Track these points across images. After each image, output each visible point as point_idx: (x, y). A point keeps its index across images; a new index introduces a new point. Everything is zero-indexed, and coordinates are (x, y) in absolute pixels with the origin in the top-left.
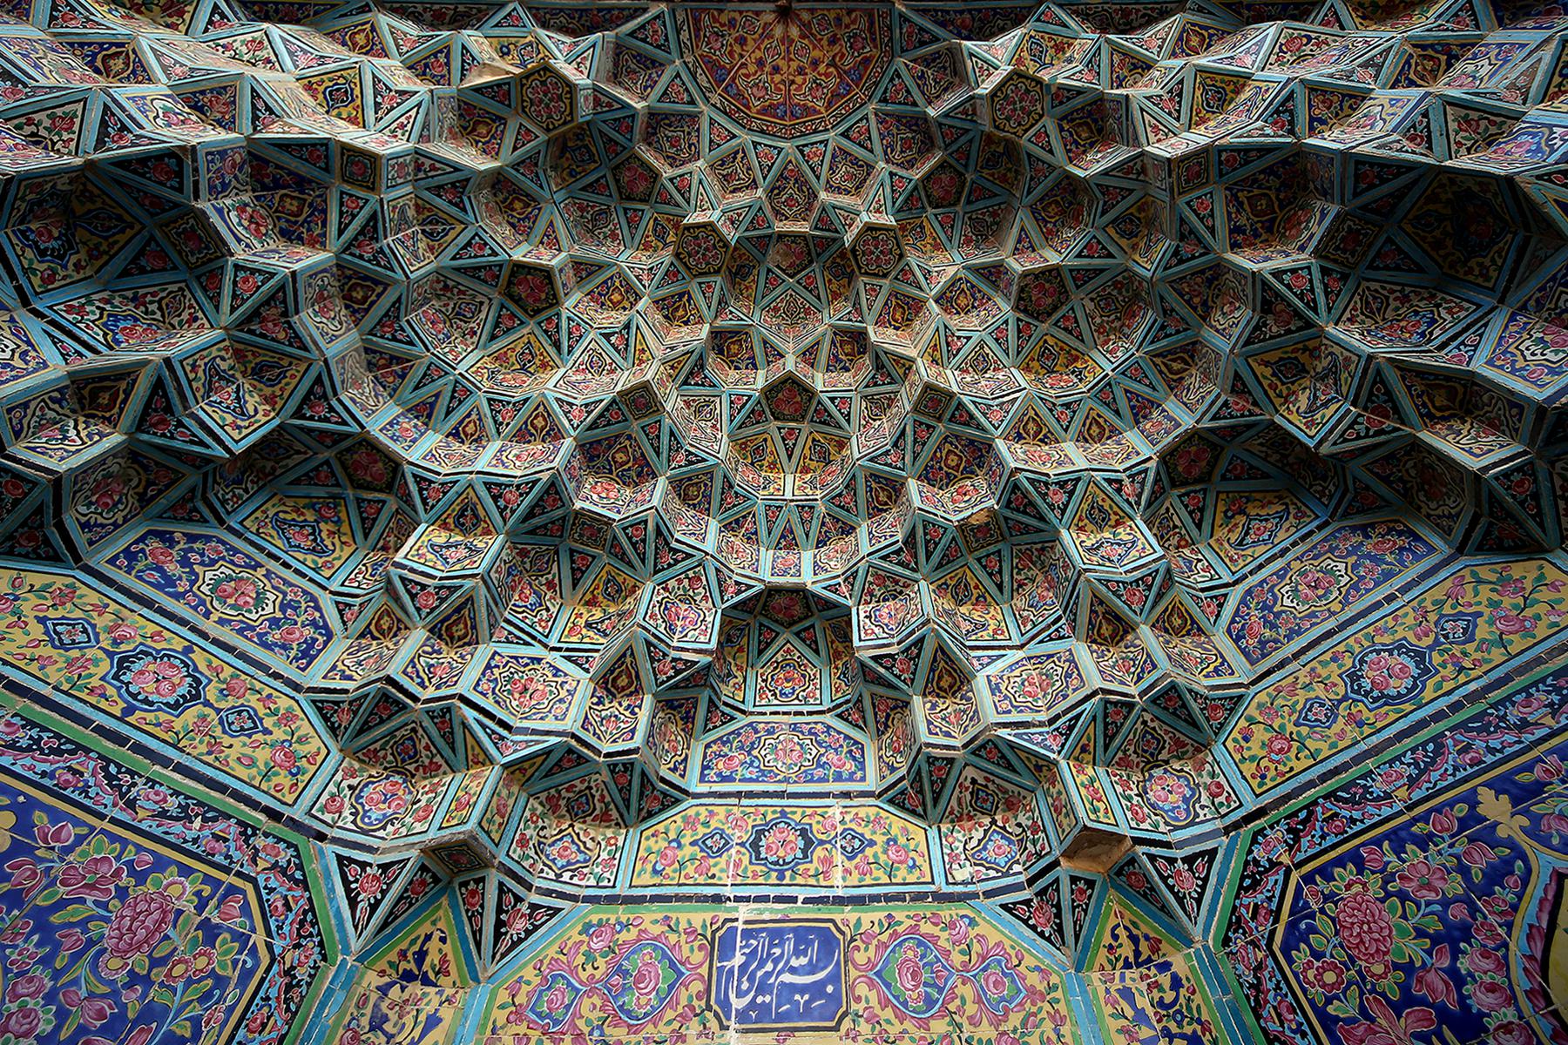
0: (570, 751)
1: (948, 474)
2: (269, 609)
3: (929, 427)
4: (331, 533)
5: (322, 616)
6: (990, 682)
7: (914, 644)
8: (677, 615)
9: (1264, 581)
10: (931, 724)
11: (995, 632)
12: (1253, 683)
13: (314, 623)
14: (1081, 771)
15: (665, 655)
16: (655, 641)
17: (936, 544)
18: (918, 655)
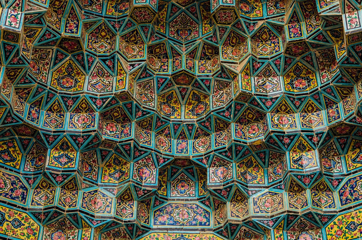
0: (114, 222)
1: (248, 120)
2: (9, 186)
3: (241, 105)
4: (13, 151)
5: (23, 184)
6: (254, 200)
7: (229, 187)
8: (143, 172)
9: (355, 178)
10: (232, 213)
11: (259, 181)
12: (340, 211)
13: (21, 187)
14: (278, 232)
15: (140, 189)
16: (137, 185)
17: (240, 152)
18: (230, 191)
